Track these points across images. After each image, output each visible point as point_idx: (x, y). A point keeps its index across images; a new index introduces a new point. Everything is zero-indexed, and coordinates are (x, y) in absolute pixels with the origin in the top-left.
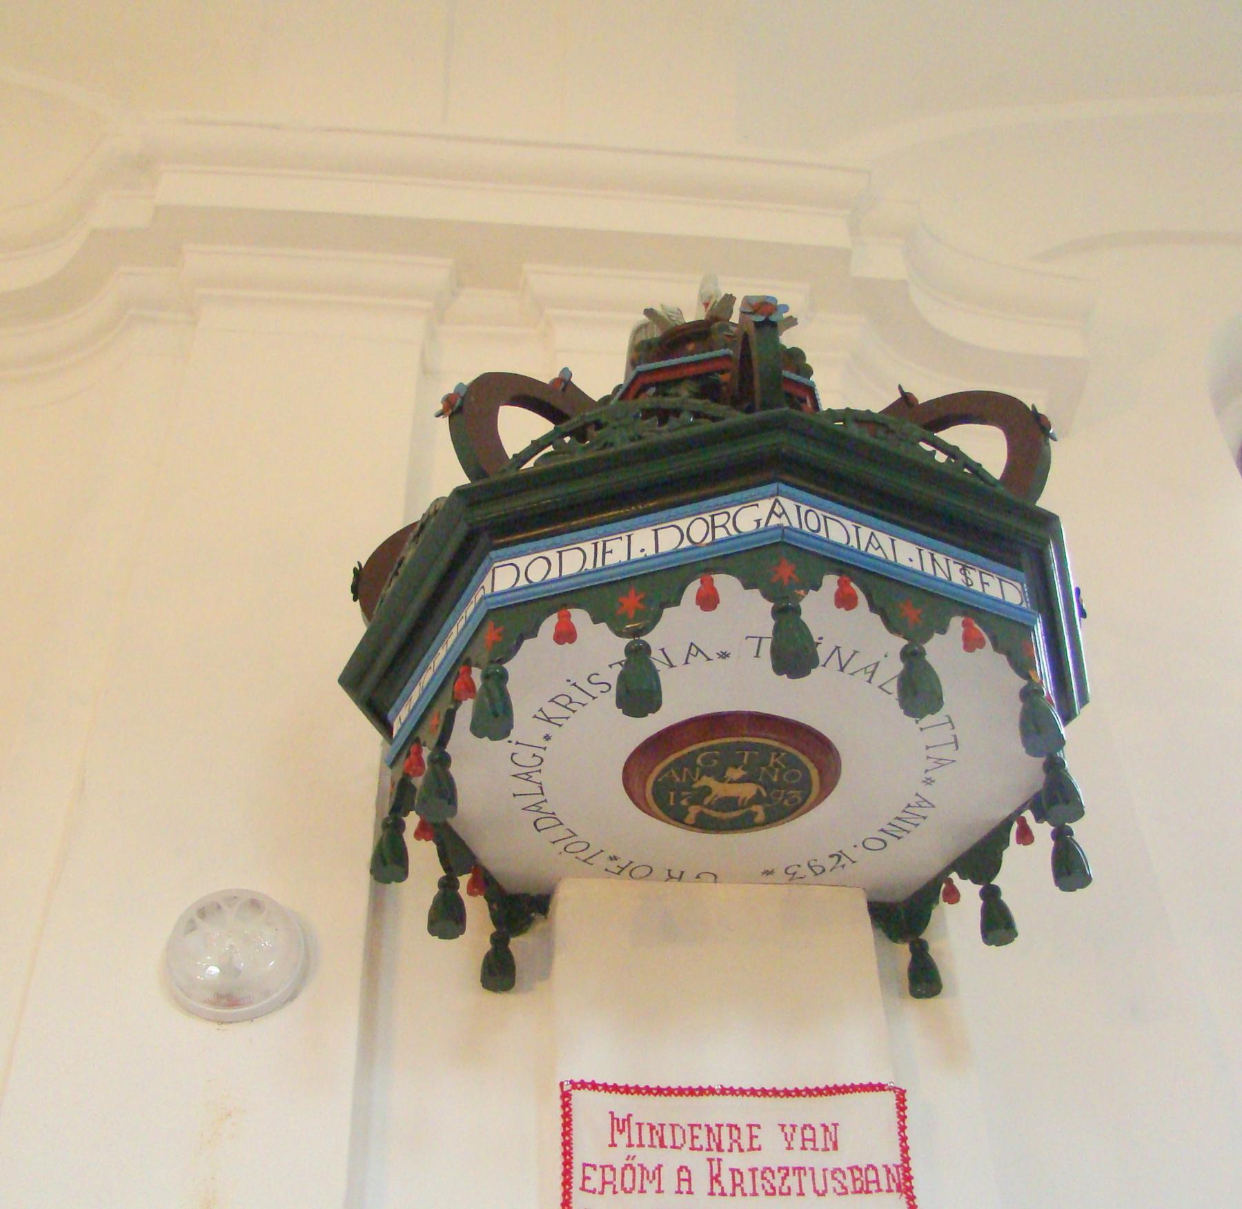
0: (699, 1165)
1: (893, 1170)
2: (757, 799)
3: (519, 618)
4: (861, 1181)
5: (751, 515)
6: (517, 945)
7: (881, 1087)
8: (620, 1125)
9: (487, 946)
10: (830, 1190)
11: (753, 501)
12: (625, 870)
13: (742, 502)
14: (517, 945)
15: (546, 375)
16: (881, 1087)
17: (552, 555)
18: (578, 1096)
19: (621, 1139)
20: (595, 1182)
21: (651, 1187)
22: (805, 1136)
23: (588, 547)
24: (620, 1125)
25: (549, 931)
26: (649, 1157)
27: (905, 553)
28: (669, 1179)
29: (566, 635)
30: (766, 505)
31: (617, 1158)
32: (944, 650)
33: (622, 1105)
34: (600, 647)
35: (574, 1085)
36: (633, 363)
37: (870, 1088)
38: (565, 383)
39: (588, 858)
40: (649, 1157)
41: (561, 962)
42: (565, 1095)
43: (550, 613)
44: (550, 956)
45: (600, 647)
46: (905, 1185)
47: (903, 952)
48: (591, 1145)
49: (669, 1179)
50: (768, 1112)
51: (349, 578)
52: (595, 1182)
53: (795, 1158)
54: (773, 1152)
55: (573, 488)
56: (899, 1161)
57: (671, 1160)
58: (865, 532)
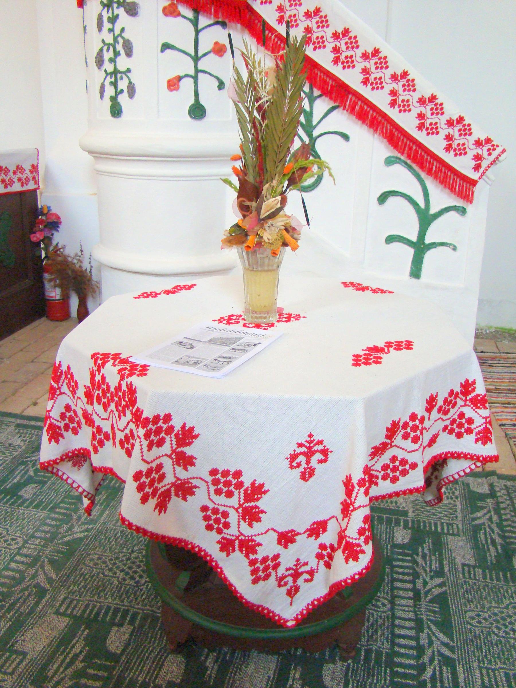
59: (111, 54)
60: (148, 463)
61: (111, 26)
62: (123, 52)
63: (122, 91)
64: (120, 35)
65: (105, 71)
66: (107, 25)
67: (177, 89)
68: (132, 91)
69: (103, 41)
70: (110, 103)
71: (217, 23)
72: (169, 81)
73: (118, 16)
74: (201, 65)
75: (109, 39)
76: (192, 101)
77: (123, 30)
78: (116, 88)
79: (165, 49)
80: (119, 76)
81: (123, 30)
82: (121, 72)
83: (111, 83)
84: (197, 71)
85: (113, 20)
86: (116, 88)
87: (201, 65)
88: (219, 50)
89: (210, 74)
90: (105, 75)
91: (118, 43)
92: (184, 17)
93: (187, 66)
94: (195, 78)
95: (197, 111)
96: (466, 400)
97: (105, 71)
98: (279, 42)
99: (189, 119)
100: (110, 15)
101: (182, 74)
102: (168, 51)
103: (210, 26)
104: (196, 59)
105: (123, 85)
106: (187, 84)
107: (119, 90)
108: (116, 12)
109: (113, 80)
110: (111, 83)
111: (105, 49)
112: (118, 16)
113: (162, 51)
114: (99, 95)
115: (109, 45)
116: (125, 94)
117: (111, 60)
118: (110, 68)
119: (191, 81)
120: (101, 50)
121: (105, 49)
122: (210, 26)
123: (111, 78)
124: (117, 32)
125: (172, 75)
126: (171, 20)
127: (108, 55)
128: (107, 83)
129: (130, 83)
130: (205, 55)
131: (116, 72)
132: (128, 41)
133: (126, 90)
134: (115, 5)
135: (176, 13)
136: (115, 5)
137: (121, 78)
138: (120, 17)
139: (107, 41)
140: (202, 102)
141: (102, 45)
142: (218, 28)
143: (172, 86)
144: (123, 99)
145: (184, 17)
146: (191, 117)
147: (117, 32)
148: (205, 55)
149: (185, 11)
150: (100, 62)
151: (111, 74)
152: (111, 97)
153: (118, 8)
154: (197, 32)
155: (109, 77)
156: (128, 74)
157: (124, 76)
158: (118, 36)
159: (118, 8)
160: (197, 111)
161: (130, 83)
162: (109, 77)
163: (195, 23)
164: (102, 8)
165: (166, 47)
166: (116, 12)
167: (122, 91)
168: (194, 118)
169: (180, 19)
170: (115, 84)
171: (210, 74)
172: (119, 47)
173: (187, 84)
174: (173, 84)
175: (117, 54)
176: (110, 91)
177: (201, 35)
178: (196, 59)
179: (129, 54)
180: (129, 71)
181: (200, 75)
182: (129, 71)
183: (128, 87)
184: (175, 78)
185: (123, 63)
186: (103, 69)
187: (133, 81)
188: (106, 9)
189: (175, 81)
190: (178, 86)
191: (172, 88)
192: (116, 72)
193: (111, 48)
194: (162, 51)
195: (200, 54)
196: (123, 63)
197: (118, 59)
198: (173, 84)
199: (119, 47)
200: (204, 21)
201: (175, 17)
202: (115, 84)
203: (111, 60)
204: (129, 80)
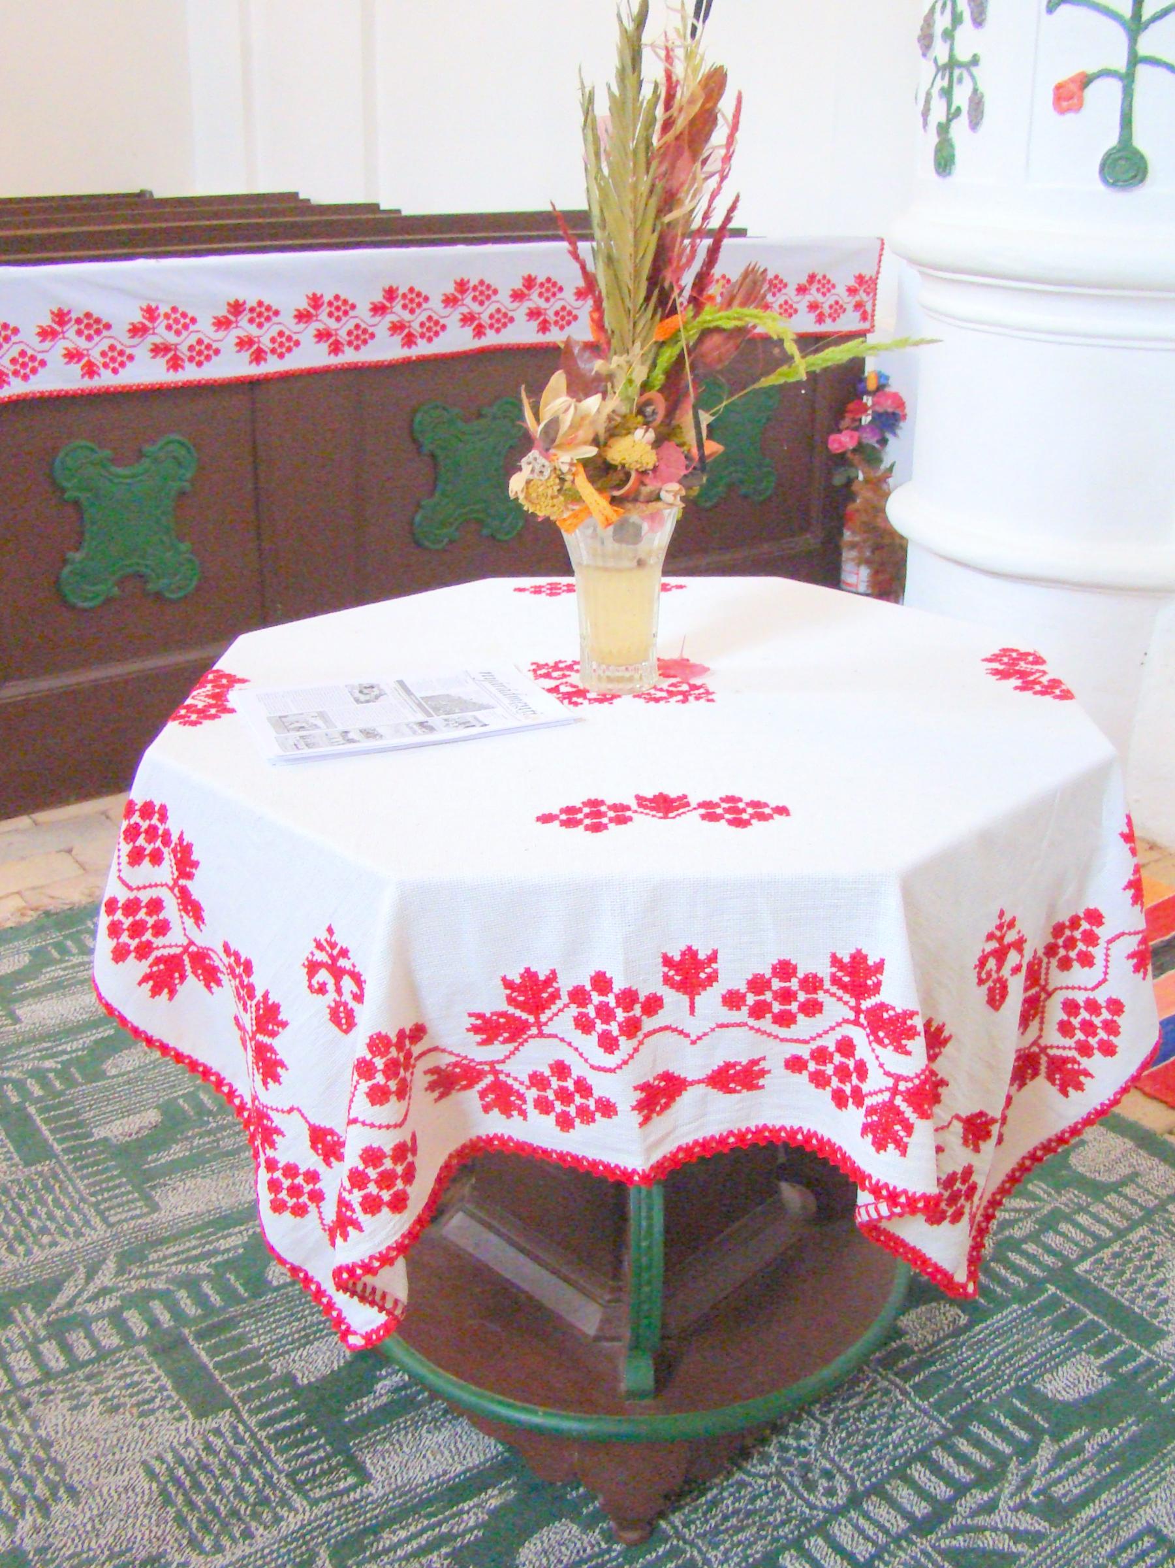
60: (130, 888)
62: (967, 16)
65: (935, 61)
72: (1058, 88)
74: (1145, 47)
76: (1112, 139)
80: (957, 72)
84: (1134, 60)
87: (1145, 47)
90: (933, 70)
94: (1128, 80)
95: (1125, 167)
96: (857, 1010)
99: (1101, 187)
101: (1091, 70)
105: (961, 97)
106: (1104, 98)
107: (953, 110)
109: (945, 84)
125: (1065, 73)
127: (942, 22)
128: (935, 92)
129: (975, 91)
131: (952, 64)
133: (965, 108)
137: (960, 81)
140: (1140, 142)
146: (1105, 181)
150: (926, 41)
152: (940, 124)
156: (974, 70)
160: (1125, 167)
161: (975, 91)
168: (1114, 185)
170: (947, 93)
173: (1104, 98)
174: (1069, 95)
175: (957, 19)
176: (938, 113)
180: (975, 61)
181: (1142, 71)
182: (975, 61)
183: (971, 100)
184: (1072, 80)
185: (968, 41)
187: (981, 89)
189: (1073, 87)
191: (1065, 104)
195: (1146, 16)
197: (959, 34)
198: (1069, 95)
204: (975, 83)
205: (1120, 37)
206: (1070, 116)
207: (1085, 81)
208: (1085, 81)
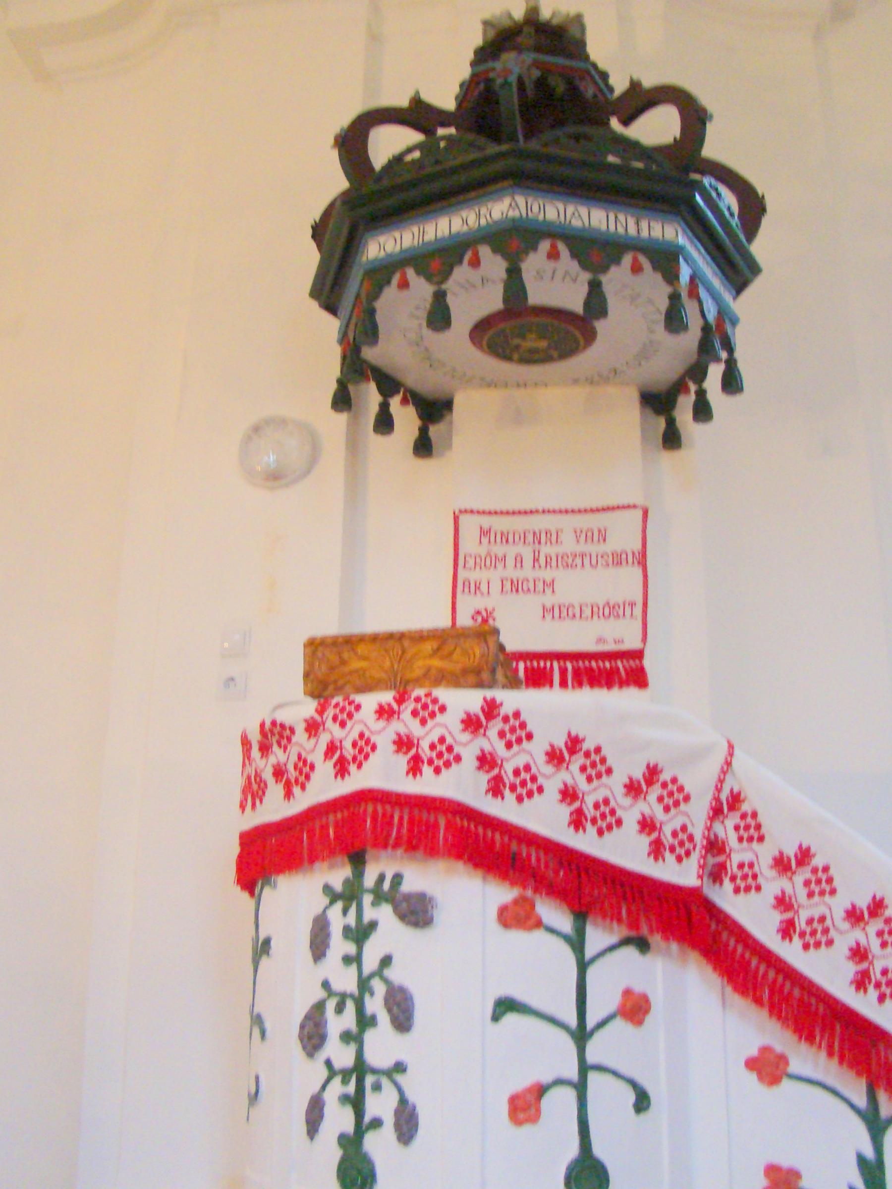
0: (527, 554)
1: (637, 554)
2: (549, 347)
3: (382, 274)
4: (618, 560)
5: (502, 208)
6: (434, 431)
7: (635, 507)
8: (484, 532)
9: (416, 433)
10: (599, 563)
11: (500, 199)
12: (491, 384)
13: (495, 201)
14: (434, 431)
15: (403, 101)
16: (635, 507)
17: (397, 235)
18: (464, 519)
19: (485, 540)
20: (471, 562)
21: (500, 566)
22: (588, 536)
23: (415, 229)
24: (484, 532)
25: (451, 423)
26: (499, 550)
27: (597, 218)
28: (510, 562)
29: (404, 284)
30: (507, 201)
31: (483, 551)
32: (616, 279)
33: (486, 521)
34: (421, 290)
35: (461, 512)
36: (473, 64)
37: (629, 507)
38: (417, 102)
39: (468, 381)
40: (499, 550)
41: (456, 441)
42: (456, 520)
43: (394, 273)
44: (450, 437)
45: (421, 290)
46: (642, 560)
47: (661, 423)
48: (470, 544)
49: (510, 562)
50: (567, 523)
51: (310, 232)
52: (471, 562)
53: (582, 547)
54: (569, 545)
55: (403, 196)
56: (638, 546)
57: (511, 551)
58: (570, 209)
59: (348, 1020)
61: (351, 948)
62: (384, 1018)
63: (377, 1123)
64: (379, 973)
65: (328, 1063)
66: (339, 946)
67: (535, 1118)
68: (407, 1123)
69: (326, 985)
70: (337, 1154)
71: (625, 942)
73: (373, 925)
75: (346, 980)
76: (573, 1150)
77: (386, 961)
78: (359, 1113)
79: (503, 1013)
80: (369, 1080)
81: (386, 961)
82: (374, 1071)
83: (345, 1099)
84: (584, 1068)
85: (361, 933)
86: (359, 1113)
88: (635, 1008)
89: (615, 1073)
90: (324, 1073)
91: (372, 994)
92: (551, 930)
93: (558, 1057)
94: (581, 1087)
97: (328, 1063)
98: (788, 986)
100: (351, 919)
101: (546, 1079)
102: (511, 1019)
103: (612, 948)
104: (581, 1036)
105: (381, 1104)
106: (560, 1105)
107: (367, 1119)
108: (369, 914)
109: (351, 1088)
110: (345, 1099)
111: (331, 1005)
112: (373, 925)
113: (496, 1018)
114: (301, 1127)
115: (343, 998)
116: (388, 1129)
117: (346, 1037)
118: (344, 1057)
119: (568, 1096)
120: (319, 1007)
121: (331, 1005)
122: (612, 948)
123: (345, 1081)
124: (370, 963)
125: (520, 1083)
126: (518, 938)
127: (338, 1023)
129: (403, 1101)
130: (601, 1024)
131: (360, 1068)
132: (402, 990)
133: (389, 1120)
134: (367, 899)
135: (532, 922)
136: (367, 899)
137: (377, 1087)
138: (380, 928)
139: (338, 985)
140: (599, 1150)
141: (321, 994)
142: (630, 953)
143: (524, 1110)
144: (380, 1146)
145: (551, 930)
147: (370, 963)
148: (601, 1024)
149: (555, 914)
150: (312, 1035)
151: (346, 1075)
153: (374, 904)
154: (583, 966)
155: (337, 1080)
156: (399, 1078)
157: (385, 1081)
158: (371, 976)
159: (374, 904)
161: (403, 1101)
162: (337, 1080)
163: (577, 943)
164: (326, 901)
165: (506, 1006)
166: (369, 914)
167: (377, 1123)
169: (539, 935)
170: (357, 1102)
171: (615, 1073)
172: (375, 1005)
173: (560, 1105)
174: (525, 1106)
175: (365, 1021)
176: (338, 1120)
177: (591, 973)
178: (581, 1036)
179: (402, 1021)
180: (401, 1067)
181: (593, 1078)
183: (398, 1113)
184: (529, 1090)
185: (382, 1045)
186: (322, 1055)
188: (339, 905)
189: (531, 1098)
190: (538, 1110)
191: (521, 1116)
192: (360, 1068)
193: (350, 1006)
194: (496, 1018)
195: (590, 1023)
196: (382, 1045)
197: (370, 1036)
198: (525, 1106)
199: (375, 1005)
200: (597, 937)
201: (530, 928)
202: (357, 1102)
203: (346, 1037)
205: (569, 1046)
206: (527, 1128)
207: (540, 1090)
208: (540, 1090)
